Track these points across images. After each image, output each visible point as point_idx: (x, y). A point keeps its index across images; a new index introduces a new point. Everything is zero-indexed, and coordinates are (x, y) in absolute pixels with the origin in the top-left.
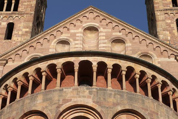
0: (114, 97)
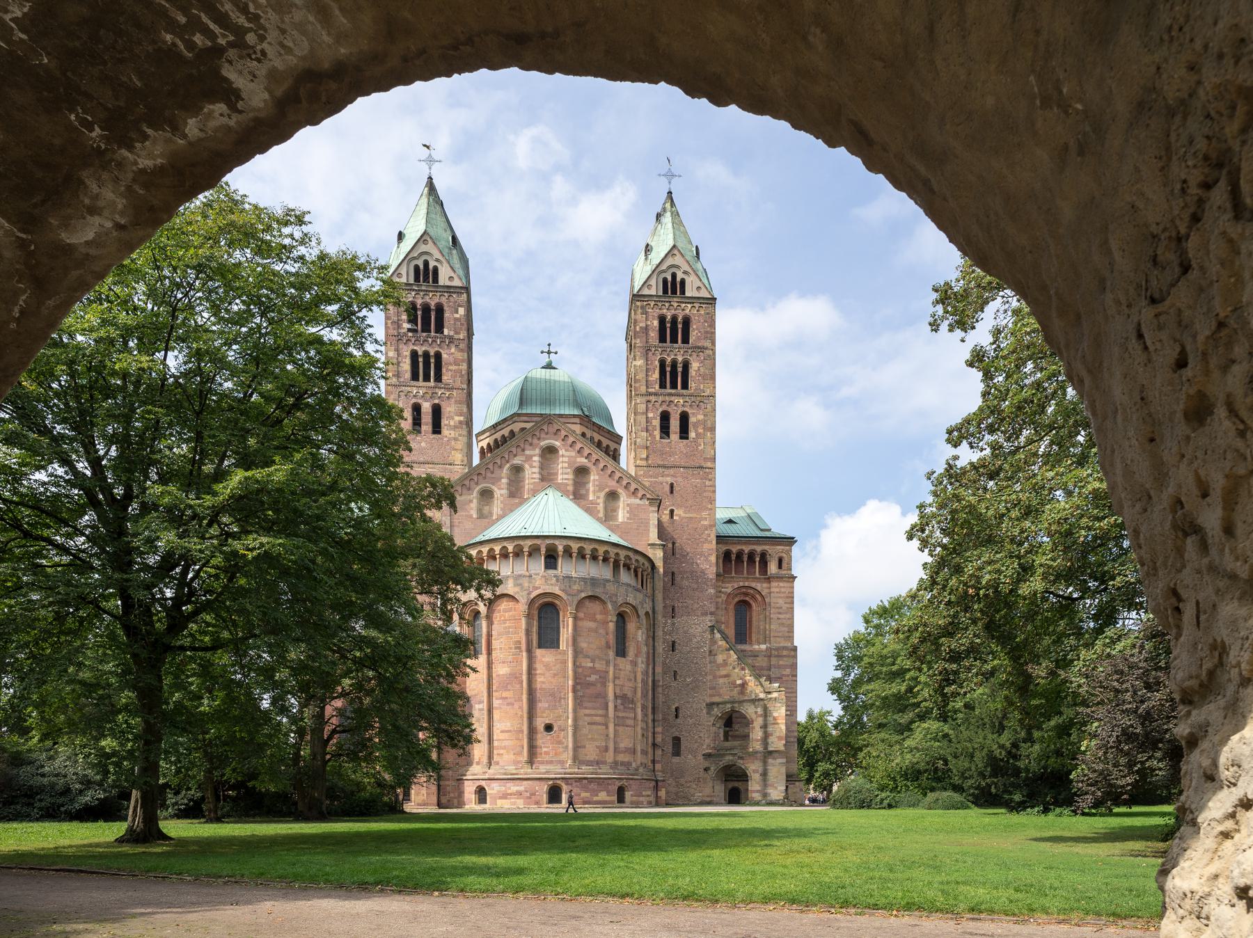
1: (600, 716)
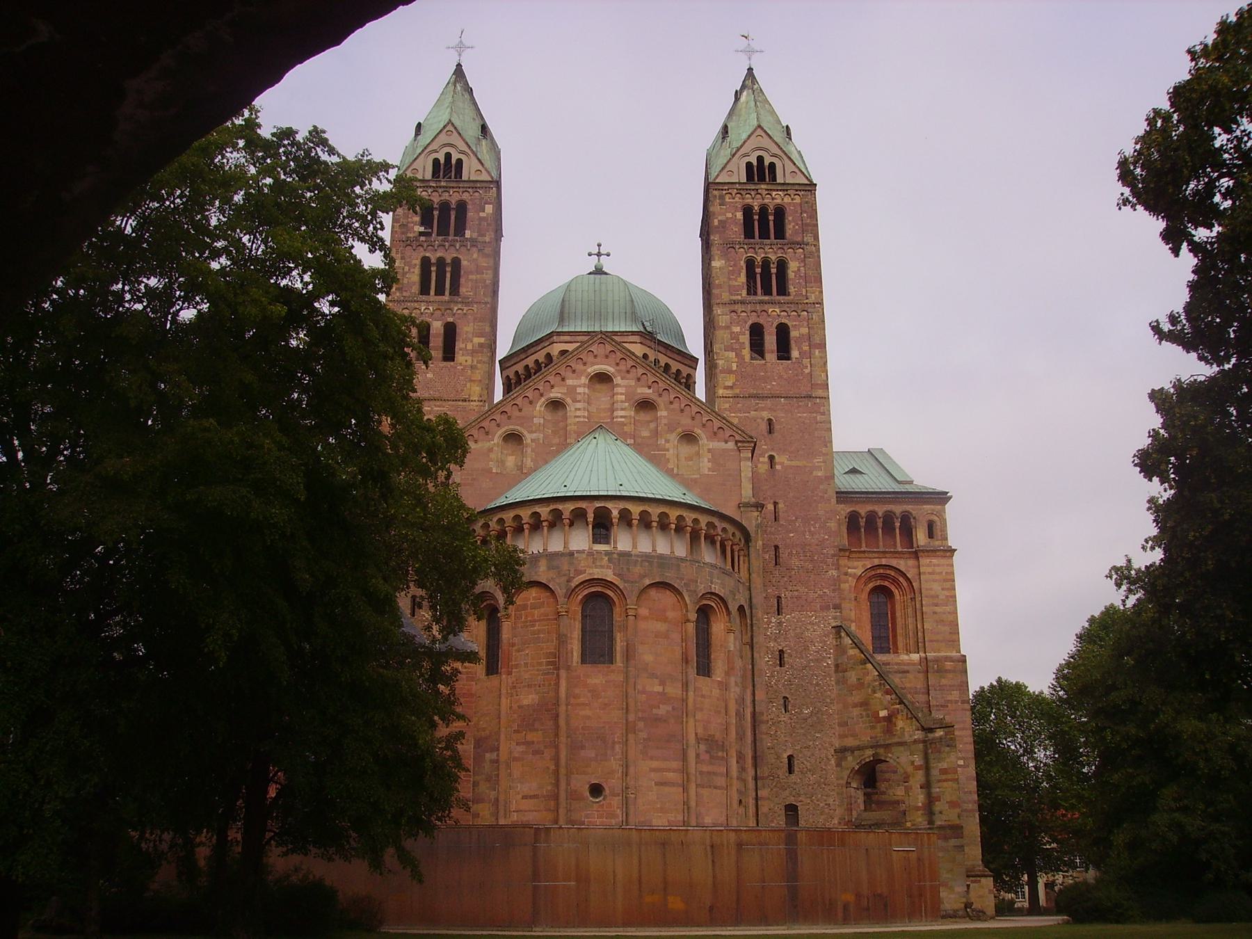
0: (641, 566)
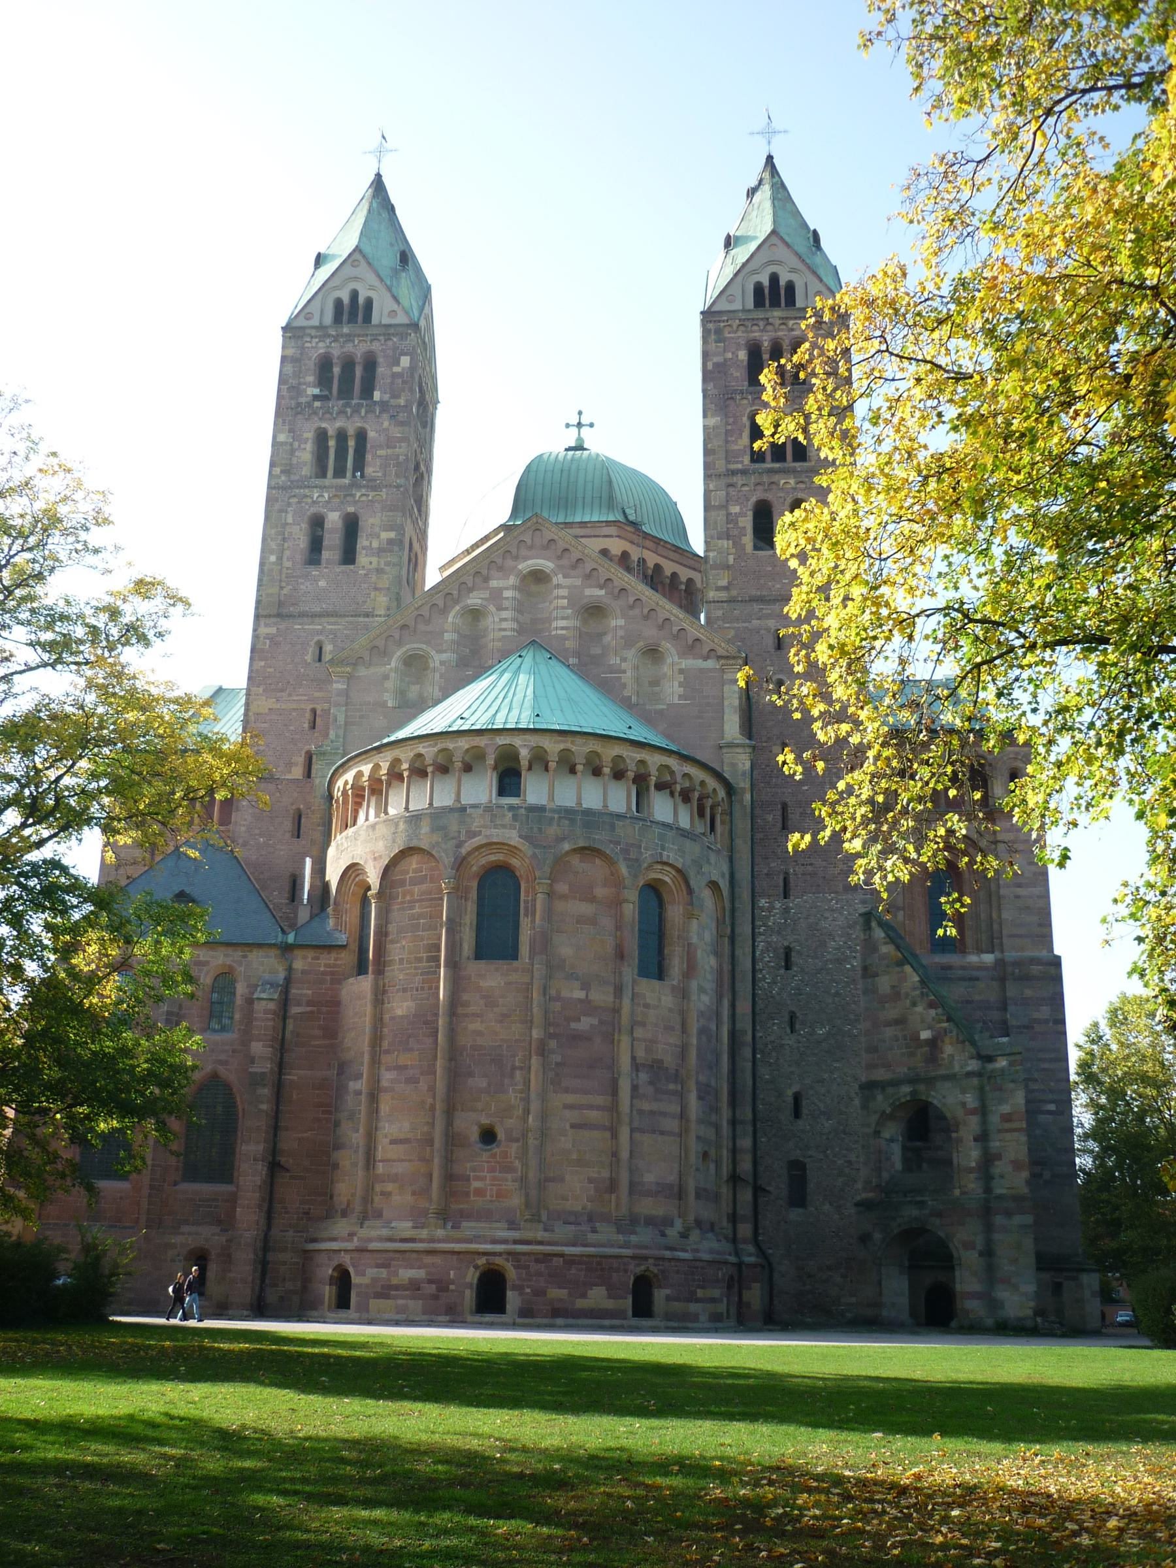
0: (558, 825)
1: (598, 1108)
